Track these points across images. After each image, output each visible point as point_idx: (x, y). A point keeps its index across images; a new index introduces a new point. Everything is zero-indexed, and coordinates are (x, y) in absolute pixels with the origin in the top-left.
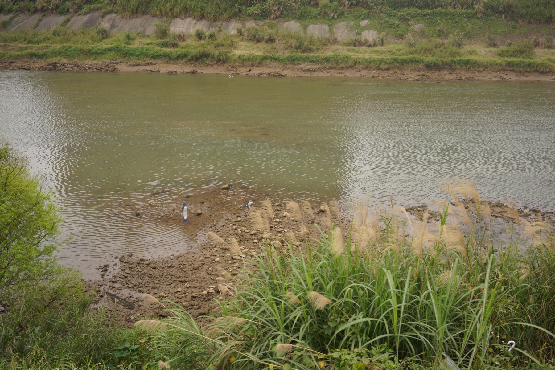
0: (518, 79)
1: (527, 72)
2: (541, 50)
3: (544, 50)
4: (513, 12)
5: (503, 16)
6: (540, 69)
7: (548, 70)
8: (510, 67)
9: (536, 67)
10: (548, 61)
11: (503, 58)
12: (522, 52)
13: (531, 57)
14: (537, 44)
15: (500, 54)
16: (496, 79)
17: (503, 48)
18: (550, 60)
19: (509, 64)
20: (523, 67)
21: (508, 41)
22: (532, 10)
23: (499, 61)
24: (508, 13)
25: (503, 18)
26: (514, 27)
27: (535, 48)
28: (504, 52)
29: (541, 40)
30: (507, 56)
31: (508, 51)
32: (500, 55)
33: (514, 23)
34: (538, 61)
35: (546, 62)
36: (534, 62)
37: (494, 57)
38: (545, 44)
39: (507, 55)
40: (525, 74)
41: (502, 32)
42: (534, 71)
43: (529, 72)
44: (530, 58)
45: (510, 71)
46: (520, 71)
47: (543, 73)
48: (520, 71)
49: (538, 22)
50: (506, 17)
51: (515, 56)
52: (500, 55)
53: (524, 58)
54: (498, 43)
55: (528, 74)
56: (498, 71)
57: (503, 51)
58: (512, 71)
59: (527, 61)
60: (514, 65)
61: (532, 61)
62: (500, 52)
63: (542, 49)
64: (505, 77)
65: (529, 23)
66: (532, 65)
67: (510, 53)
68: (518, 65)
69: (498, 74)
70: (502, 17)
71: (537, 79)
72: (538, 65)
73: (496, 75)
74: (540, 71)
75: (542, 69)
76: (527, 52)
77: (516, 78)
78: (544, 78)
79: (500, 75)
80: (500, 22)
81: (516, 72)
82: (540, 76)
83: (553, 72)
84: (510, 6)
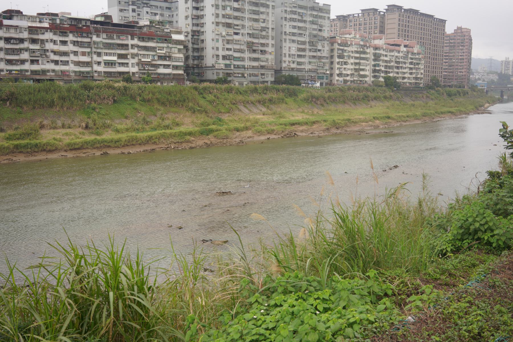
0: (27, 159)
1: (35, 152)
2: (47, 131)
3: (49, 131)
4: (16, 99)
5: (8, 103)
6: (47, 148)
7: (54, 148)
8: (18, 149)
9: (43, 147)
10: (53, 141)
11: (11, 142)
12: (29, 134)
13: (37, 138)
14: (42, 127)
15: (7, 138)
16: (5, 162)
17: (11, 132)
18: (55, 139)
19: (17, 147)
20: (30, 148)
21: (15, 125)
22: (34, 96)
23: (6, 145)
24: (11, 100)
25: (8, 105)
26: (20, 113)
27: (41, 129)
28: (11, 136)
29: (45, 122)
30: (15, 140)
31: (15, 135)
32: (8, 139)
33: (19, 109)
34: (44, 141)
35: (51, 141)
36: (40, 143)
37: (2, 142)
38: (50, 125)
39: (15, 138)
40: (33, 154)
41: (8, 117)
42: (41, 151)
43: (37, 152)
44: (37, 139)
45: (18, 152)
46: (28, 152)
47: (50, 151)
48: (28, 152)
49: (42, 106)
50: (10, 104)
51: (23, 139)
52: (8, 139)
53: (30, 140)
54: (5, 128)
55: (36, 154)
56: (7, 154)
57: (10, 135)
58: (21, 152)
59: (34, 142)
60: (21, 147)
61: (38, 141)
62: (7, 136)
63: (48, 130)
64: (14, 159)
65: (34, 108)
66: (39, 145)
67: (17, 136)
68: (26, 146)
69: (8, 157)
70: (7, 105)
71: (45, 157)
72: (44, 145)
73: (5, 158)
74: (47, 150)
75: (49, 148)
76: (33, 134)
77: (25, 159)
78: (51, 156)
79: (9, 157)
80: (5, 109)
81: (24, 153)
82: (47, 154)
83: (59, 150)
84: (12, 94)
